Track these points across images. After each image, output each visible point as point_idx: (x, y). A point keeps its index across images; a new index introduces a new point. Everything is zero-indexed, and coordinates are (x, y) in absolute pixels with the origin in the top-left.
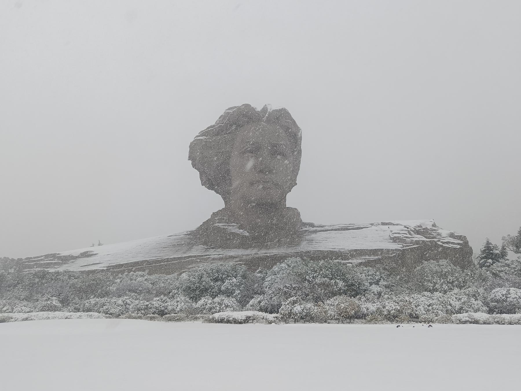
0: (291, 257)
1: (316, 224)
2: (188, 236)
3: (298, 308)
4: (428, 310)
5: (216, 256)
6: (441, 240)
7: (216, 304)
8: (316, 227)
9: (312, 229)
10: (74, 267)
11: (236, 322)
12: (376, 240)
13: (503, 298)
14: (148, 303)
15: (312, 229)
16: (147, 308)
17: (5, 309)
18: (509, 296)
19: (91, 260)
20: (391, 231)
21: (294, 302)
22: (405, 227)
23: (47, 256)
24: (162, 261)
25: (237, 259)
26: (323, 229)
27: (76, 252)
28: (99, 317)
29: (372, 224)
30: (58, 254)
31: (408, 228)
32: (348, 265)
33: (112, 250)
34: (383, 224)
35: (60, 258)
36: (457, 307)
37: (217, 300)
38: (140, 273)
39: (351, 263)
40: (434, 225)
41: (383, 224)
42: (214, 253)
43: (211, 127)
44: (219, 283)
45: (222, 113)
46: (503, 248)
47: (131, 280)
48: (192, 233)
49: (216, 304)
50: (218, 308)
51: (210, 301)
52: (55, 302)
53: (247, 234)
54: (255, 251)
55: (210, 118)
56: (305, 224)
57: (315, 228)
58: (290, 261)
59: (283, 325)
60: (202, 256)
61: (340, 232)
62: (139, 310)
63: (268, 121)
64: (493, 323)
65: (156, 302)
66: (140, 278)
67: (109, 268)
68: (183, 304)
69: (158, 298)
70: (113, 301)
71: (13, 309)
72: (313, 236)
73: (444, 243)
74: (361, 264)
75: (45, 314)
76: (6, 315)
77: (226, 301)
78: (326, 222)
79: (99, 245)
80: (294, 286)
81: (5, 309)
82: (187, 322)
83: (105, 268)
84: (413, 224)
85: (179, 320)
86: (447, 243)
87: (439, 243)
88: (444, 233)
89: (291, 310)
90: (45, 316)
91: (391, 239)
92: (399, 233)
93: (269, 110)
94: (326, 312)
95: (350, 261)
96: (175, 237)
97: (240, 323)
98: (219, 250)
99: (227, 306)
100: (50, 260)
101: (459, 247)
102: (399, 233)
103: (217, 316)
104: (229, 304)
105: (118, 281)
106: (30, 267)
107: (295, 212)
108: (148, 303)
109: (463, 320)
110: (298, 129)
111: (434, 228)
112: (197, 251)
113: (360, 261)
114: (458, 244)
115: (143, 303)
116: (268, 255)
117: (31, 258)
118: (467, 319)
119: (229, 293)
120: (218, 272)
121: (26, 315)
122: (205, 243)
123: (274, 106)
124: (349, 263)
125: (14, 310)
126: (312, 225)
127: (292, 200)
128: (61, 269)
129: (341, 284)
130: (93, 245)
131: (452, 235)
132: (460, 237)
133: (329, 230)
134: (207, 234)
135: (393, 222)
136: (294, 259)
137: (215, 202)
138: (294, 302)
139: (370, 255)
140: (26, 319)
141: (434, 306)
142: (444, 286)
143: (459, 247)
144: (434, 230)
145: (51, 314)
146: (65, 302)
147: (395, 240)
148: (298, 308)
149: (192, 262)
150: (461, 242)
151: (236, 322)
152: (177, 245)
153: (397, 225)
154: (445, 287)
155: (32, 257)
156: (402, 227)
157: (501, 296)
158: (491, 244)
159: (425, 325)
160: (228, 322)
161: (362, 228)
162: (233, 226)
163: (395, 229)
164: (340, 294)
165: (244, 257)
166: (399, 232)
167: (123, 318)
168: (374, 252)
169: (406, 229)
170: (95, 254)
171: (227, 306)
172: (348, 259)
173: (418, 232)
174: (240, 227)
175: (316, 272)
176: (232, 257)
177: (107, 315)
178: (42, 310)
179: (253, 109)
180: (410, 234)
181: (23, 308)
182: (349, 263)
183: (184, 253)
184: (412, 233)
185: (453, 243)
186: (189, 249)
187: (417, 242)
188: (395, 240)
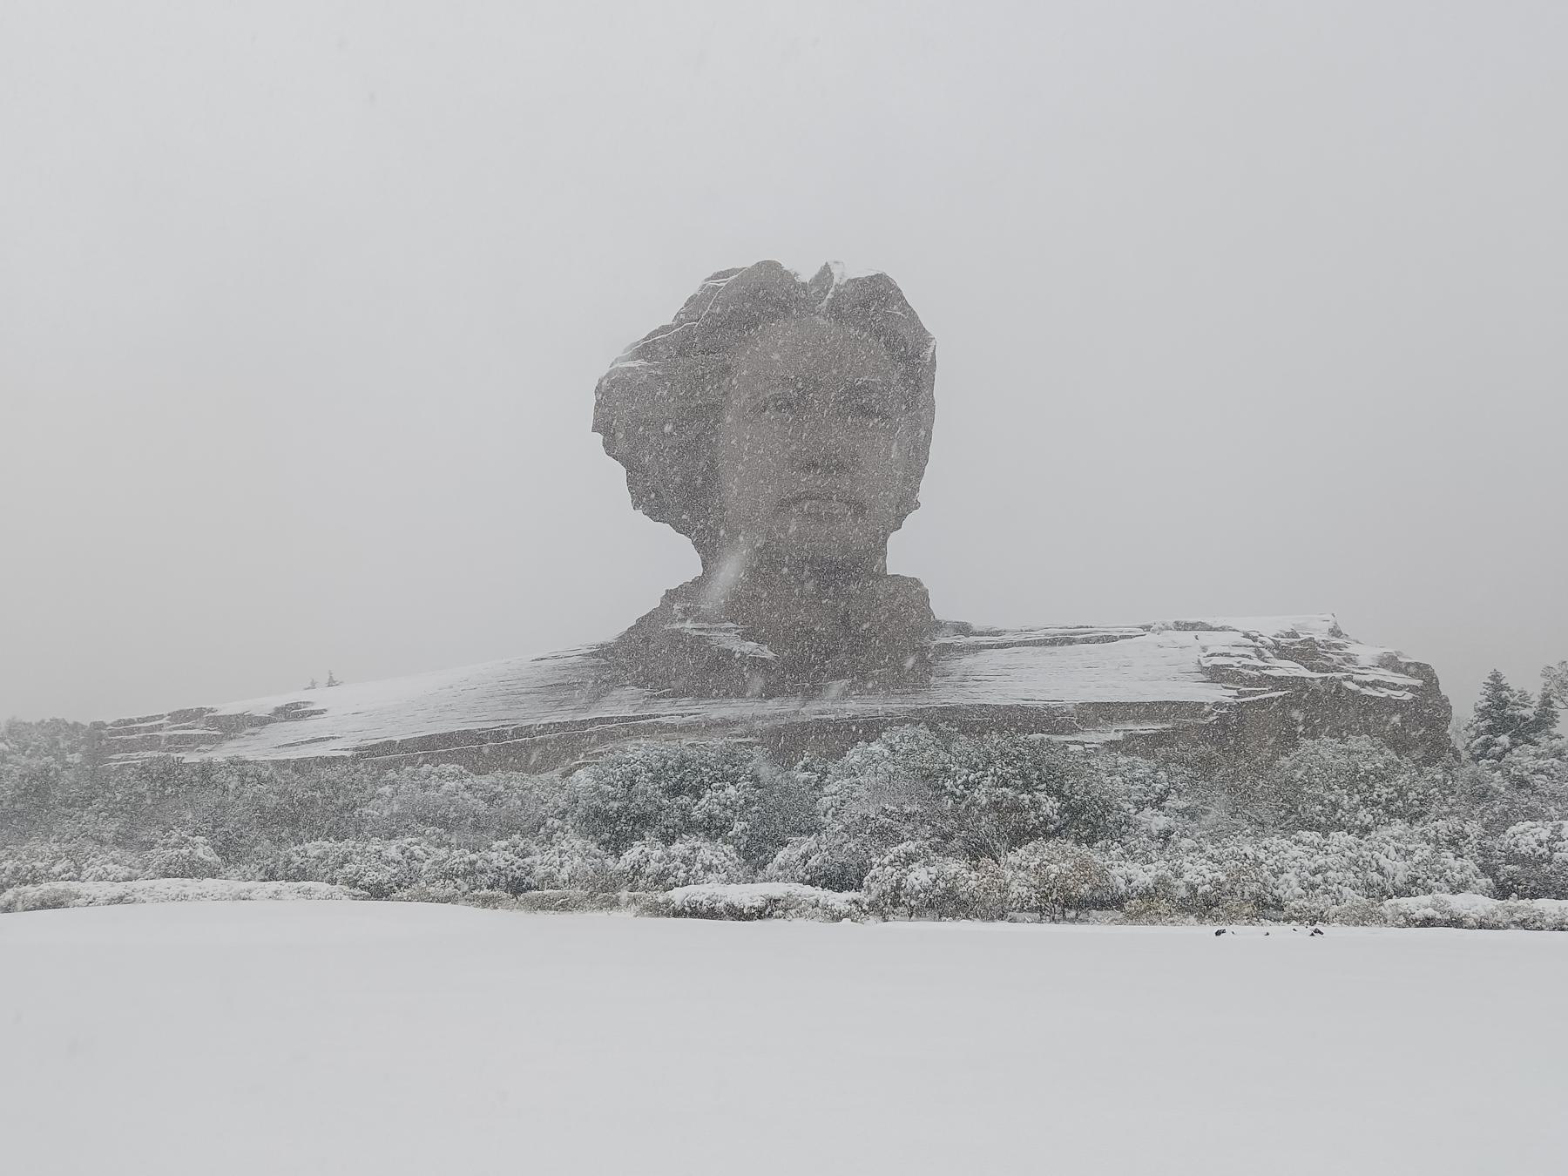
0: (902, 722)
1: (977, 625)
2: (594, 661)
3: (919, 876)
4: (1313, 886)
5: (677, 720)
6: (1356, 677)
7: (678, 862)
8: (975, 634)
9: (964, 640)
10: (257, 749)
11: (736, 913)
12: (1158, 673)
13: (1541, 850)
14: (474, 857)
15: (964, 640)
16: (471, 871)
17: (57, 869)
18: (1560, 844)
19: (307, 728)
20: (1204, 649)
21: (910, 858)
22: (1247, 636)
23: (180, 716)
24: (518, 732)
25: (739, 730)
26: (998, 641)
27: (264, 705)
28: (331, 897)
29: (1148, 628)
30: (211, 710)
32: (1072, 748)
33: (370, 698)
34: (1181, 627)
35: (216, 721)
36: (1401, 878)
37: (678, 848)
38: (450, 768)
39: (1083, 744)
41: (1181, 627)
42: (668, 711)
43: (664, 330)
44: (685, 800)
45: (694, 289)
46: (1546, 702)
47: (425, 788)
48: (603, 651)
49: (678, 862)
50: (681, 874)
51: (658, 853)
52: (203, 851)
53: (770, 655)
54: (792, 705)
55: (660, 306)
56: (939, 626)
57: (972, 639)
58: (893, 735)
59: (873, 924)
60: (638, 718)
61: (1049, 649)
62: (449, 875)
63: (836, 310)
64: (1506, 927)
65: (499, 854)
66: (450, 783)
67: (364, 753)
68: (577, 860)
69: (504, 843)
70: (372, 848)
71: (79, 869)
72: (968, 661)
73: (1364, 684)
74: (1112, 746)
75: (175, 885)
76: (61, 885)
77: (708, 852)
78: (1010, 621)
79: (331, 683)
80: (908, 809)
81: (57, 869)
82: (588, 914)
83: (348, 754)
84: (1270, 627)
85: (564, 907)
86: (1374, 684)
87: (1350, 685)
88: (1366, 654)
89: (899, 881)
90: (174, 892)
91: (1204, 670)
92: (1228, 655)
93: (836, 280)
94: (1004, 889)
95: (1079, 737)
96: (557, 662)
97: (749, 917)
98: (685, 701)
99: (708, 868)
100: (183, 728)
102: (1228, 655)
103: (678, 895)
104: (715, 862)
105: (387, 790)
106: (129, 747)
107: (913, 592)
108: (474, 857)
109: (1419, 914)
110: (923, 338)
112: (621, 704)
113: (1112, 736)
114: (1412, 689)
115: (460, 858)
116: (832, 717)
117: (131, 721)
118: (1430, 912)
119: (714, 829)
120: (682, 766)
121: (119, 889)
122: (644, 680)
123: (854, 266)
124: (1076, 743)
125: (85, 874)
126: (963, 629)
127: (905, 553)
128: (219, 755)
129: (1050, 805)
130: (313, 686)
131: (1390, 662)
133: (1014, 645)
134: (650, 654)
135: (1209, 621)
136: (908, 730)
138: (910, 858)
139: (1138, 719)
140: (121, 899)
141: (1330, 874)
142: (1360, 815)
143: (1409, 696)
144: (1337, 646)
145: (191, 885)
146: (231, 852)
147: (1216, 675)
148: (919, 876)
149: (603, 737)
150: (1418, 682)
151: (736, 913)
152: (558, 688)
153: (1223, 629)
154: (1365, 817)
155: (134, 717)
156: (1237, 638)
157: (1535, 845)
158: (1508, 689)
159: (1301, 928)
160: (712, 914)
161: (1115, 639)
162: (727, 630)
164: (1048, 836)
165: (758, 724)
166: (1226, 650)
167: (400, 899)
168: (1150, 710)
169: (1250, 642)
170: (321, 712)
171: (708, 868)
172: (1073, 730)
173: (1283, 652)
174: (746, 636)
175: (974, 768)
176: (725, 724)
177: (357, 891)
178: (167, 875)
179: (787, 277)
180: (1260, 656)
181: (110, 867)
182: (1076, 743)
183: (586, 710)
184: (1268, 654)
185: (1393, 687)
186: (598, 697)
187: (1280, 683)
188: (1216, 675)
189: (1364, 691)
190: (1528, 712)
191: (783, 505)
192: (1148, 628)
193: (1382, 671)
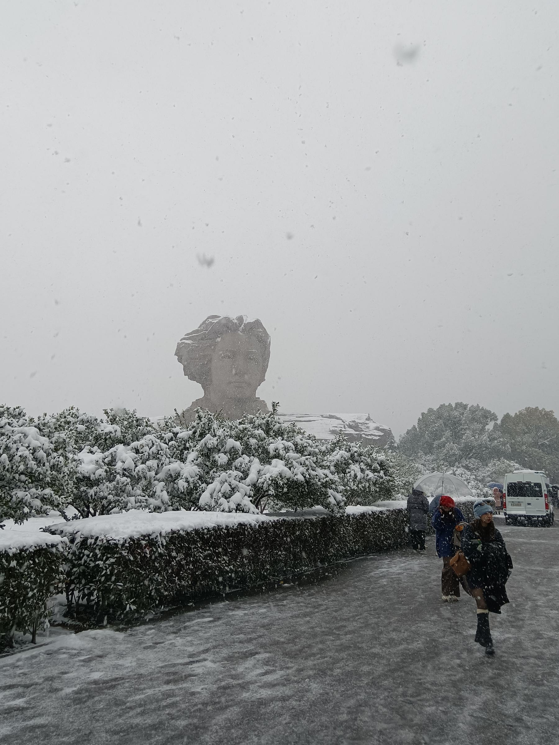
6: (366, 433)
29: (322, 416)
31: (344, 422)
34: (331, 417)
40: (368, 419)
87: (363, 436)
101: (378, 438)
111: (367, 422)
114: (379, 436)
131: (377, 429)
132: (382, 430)
137: (196, 391)
143: (378, 438)
144: (366, 424)
147: (333, 432)
163: (335, 422)
173: (350, 426)
184: (346, 427)
188: (333, 432)
189: (367, 437)
190: (396, 445)
191: (230, 383)
192: (322, 416)
193: (375, 431)
